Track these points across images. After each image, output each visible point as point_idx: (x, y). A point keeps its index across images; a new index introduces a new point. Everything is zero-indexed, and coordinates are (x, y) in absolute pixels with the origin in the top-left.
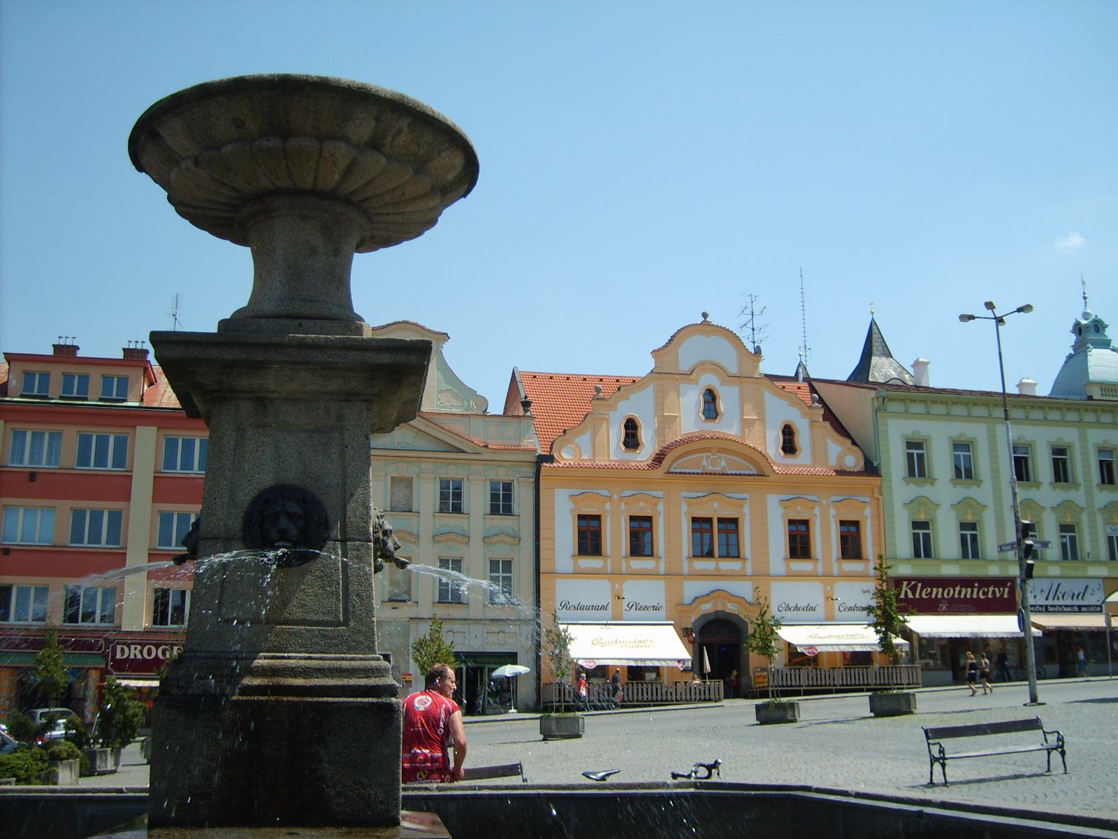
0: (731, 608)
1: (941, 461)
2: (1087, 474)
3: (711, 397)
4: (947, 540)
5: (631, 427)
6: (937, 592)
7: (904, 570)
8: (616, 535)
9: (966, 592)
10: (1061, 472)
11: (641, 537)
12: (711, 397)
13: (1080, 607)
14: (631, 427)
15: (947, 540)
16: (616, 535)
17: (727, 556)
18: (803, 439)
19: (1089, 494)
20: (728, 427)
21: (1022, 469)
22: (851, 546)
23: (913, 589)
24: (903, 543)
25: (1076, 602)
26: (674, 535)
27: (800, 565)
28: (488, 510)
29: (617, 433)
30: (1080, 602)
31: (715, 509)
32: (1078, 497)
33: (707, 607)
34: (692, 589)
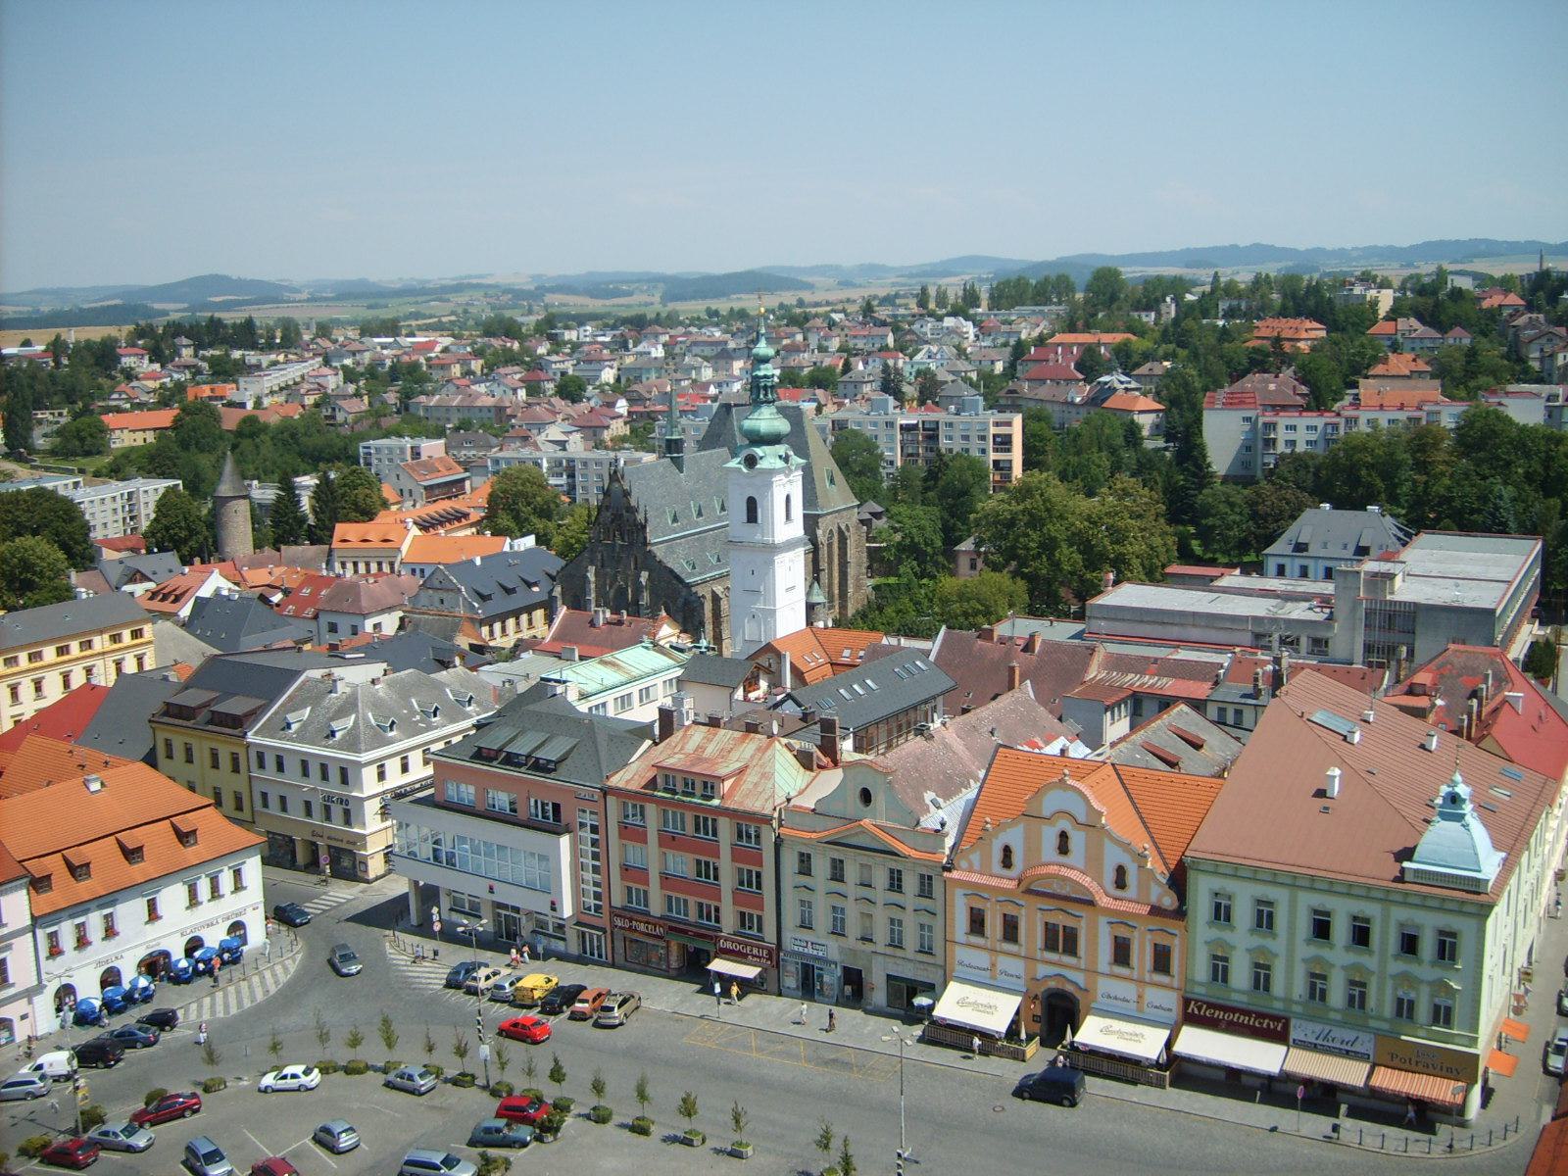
0: (1069, 988)
1: (1243, 913)
2: (1384, 942)
3: (1064, 836)
4: (1240, 976)
7: (1200, 990)
8: (994, 925)
10: (1361, 935)
11: (1011, 930)
12: (1064, 836)
13: (1348, 1052)
15: (1240, 976)
16: (994, 925)
17: (1065, 951)
19: (1383, 962)
21: (1322, 929)
22: (1162, 961)
23: (1199, 1009)
24: (1201, 971)
25: (1344, 1047)
26: (1032, 931)
28: (917, 891)
30: (1348, 1048)
31: (1060, 920)
32: (1370, 961)
33: (1052, 984)
34: (1042, 970)
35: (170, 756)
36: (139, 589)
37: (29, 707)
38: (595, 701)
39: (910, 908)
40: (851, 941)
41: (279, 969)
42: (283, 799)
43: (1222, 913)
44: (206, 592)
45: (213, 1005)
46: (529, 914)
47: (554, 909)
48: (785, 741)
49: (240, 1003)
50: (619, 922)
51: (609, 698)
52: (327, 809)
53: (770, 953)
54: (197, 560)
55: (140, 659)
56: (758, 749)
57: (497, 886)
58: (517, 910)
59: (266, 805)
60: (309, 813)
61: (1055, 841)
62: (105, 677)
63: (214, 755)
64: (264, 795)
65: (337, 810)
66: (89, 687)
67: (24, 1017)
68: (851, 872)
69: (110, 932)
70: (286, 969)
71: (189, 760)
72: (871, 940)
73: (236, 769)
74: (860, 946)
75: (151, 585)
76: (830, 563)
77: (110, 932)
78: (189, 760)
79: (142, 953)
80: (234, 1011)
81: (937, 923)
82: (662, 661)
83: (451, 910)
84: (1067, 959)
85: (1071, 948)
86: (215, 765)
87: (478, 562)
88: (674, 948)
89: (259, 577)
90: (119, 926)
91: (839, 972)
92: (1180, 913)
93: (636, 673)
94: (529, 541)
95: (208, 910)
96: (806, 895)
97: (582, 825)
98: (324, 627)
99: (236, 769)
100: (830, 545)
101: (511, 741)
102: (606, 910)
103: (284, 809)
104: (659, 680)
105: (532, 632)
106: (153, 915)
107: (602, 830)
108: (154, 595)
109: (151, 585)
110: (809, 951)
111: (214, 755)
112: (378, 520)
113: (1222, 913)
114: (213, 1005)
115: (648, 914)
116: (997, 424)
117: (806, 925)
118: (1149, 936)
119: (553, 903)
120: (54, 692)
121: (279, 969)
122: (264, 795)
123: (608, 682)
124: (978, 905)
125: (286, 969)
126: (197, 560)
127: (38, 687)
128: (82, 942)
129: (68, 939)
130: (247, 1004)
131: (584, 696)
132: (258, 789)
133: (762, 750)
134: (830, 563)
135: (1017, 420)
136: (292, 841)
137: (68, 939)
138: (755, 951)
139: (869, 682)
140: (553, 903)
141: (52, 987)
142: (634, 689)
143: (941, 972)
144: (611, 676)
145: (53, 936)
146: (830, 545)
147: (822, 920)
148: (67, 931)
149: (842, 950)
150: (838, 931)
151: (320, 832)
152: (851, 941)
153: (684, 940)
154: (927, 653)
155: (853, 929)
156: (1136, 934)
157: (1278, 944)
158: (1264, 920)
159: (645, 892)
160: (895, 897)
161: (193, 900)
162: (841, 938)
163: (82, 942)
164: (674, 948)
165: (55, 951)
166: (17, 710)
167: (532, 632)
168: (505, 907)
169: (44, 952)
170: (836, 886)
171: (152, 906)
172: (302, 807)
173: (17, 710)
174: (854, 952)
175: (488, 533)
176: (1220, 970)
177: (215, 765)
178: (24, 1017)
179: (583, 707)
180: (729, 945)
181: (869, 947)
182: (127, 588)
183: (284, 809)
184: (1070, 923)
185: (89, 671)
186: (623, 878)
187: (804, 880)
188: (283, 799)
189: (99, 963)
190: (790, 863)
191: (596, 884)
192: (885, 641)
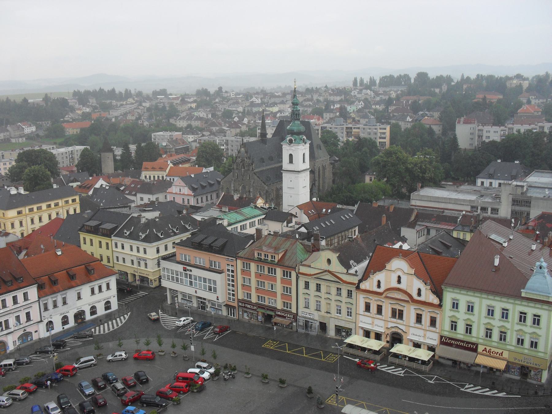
0: (400, 331)
3: (399, 277)
4: (461, 328)
5: (379, 282)
6: (453, 342)
7: (446, 334)
8: (373, 308)
9: (462, 344)
11: (379, 310)
12: (399, 277)
14: (379, 282)
16: (373, 308)
17: (398, 319)
18: (423, 293)
20: (402, 286)
22: (433, 322)
23: (446, 340)
24: (447, 326)
27: (418, 325)
28: (347, 296)
29: (376, 284)
31: (398, 307)
33: (394, 330)
34: (390, 325)
35: (85, 243)
36: (75, 185)
37: (37, 225)
38: (233, 226)
39: (344, 302)
40: (323, 313)
41: (122, 318)
42: (124, 259)
43: (455, 306)
44: (97, 186)
45: (100, 330)
46: (209, 301)
47: (218, 299)
48: (300, 241)
49: (109, 329)
50: (240, 304)
51: (239, 225)
52: (139, 263)
53: (294, 317)
54: (95, 175)
55: (75, 210)
56: (291, 244)
57: (198, 290)
58: (205, 299)
59: (118, 261)
60: (133, 264)
61: (396, 279)
62: (64, 216)
63: (100, 242)
64: (117, 257)
65: (142, 263)
66: (57, 219)
67: (36, 332)
68: (323, 288)
69: (65, 303)
70: (125, 318)
71: (92, 245)
72: (329, 313)
73: (108, 248)
74: (326, 315)
75: (79, 183)
76: (319, 178)
77: (65, 303)
78: (92, 245)
79: (76, 311)
80: (107, 331)
81: (354, 308)
82: (258, 212)
83: (182, 299)
84: (399, 321)
85: (401, 316)
86: (101, 247)
87: (193, 176)
88: (260, 314)
89: (116, 181)
90: (68, 301)
91: (318, 324)
92: (440, 306)
93: (249, 216)
94: (212, 169)
95: (98, 296)
96: (307, 296)
97: (228, 270)
98: (139, 199)
99: (108, 248)
100: (319, 172)
101: (204, 240)
102: (236, 300)
103: (124, 262)
104: (256, 219)
105: (212, 201)
106: (79, 298)
107: (235, 272)
108: (80, 187)
109: (79, 183)
110: (308, 316)
111: (100, 242)
112: (158, 161)
113: (455, 306)
114: (100, 330)
115: (251, 302)
116: (381, 129)
117: (307, 307)
118: (429, 314)
119: (218, 297)
120: (46, 221)
121: (122, 318)
122: (117, 257)
123: (238, 220)
124: (368, 301)
125: (125, 318)
126: (95, 175)
127: (40, 219)
128: (55, 306)
129: (50, 306)
130: (111, 329)
131: (230, 225)
132: (115, 255)
133: (292, 244)
134: (319, 178)
135: (388, 128)
136: (127, 274)
137: (50, 306)
138: (289, 316)
139: (331, 221)
140: (218, 297)
141: (46, 321)
142: (248, 222)
143: (354, 324)
144: (240, 218)
145: (46, 305)
146: (319, 172)
147: (313, 305)
148: (50, 301)
149: (319, 316)
150: (318, 310)
151: (136, 270)
152: (323, 313)
153: (263, 311)
154: (352, 211)
155: (324, 308)
156: (424, 313)
157: (474, 318)
158: (470, 308)
159: (250, 294)
160: (338, 298)
162: (319, 312)
163: (55, 306)
164: (260, 314)
165: (46, 309)
166: (33, 226)
167: (212, 201)
168: (201, 298)
170: (318, 294)
171: (79, 294)
172: (130, 262)
173: (33, 226)
174: (323, 317)
175: (197, 166)
176: (454, 326)
177: (101, 247)
178: (36, 332)
179: (229, 228)
180: (279, 313)
181: (329, 315)
182: (71, 184)
183: (124, 262)
184: (401, 308)
185: (57, 214)
186: (242, 289)
187: (306, 291)
188: (124, 259)
189: (61, 314)
190: (302, 284)
191: (233, 291)
192: (338, 206)
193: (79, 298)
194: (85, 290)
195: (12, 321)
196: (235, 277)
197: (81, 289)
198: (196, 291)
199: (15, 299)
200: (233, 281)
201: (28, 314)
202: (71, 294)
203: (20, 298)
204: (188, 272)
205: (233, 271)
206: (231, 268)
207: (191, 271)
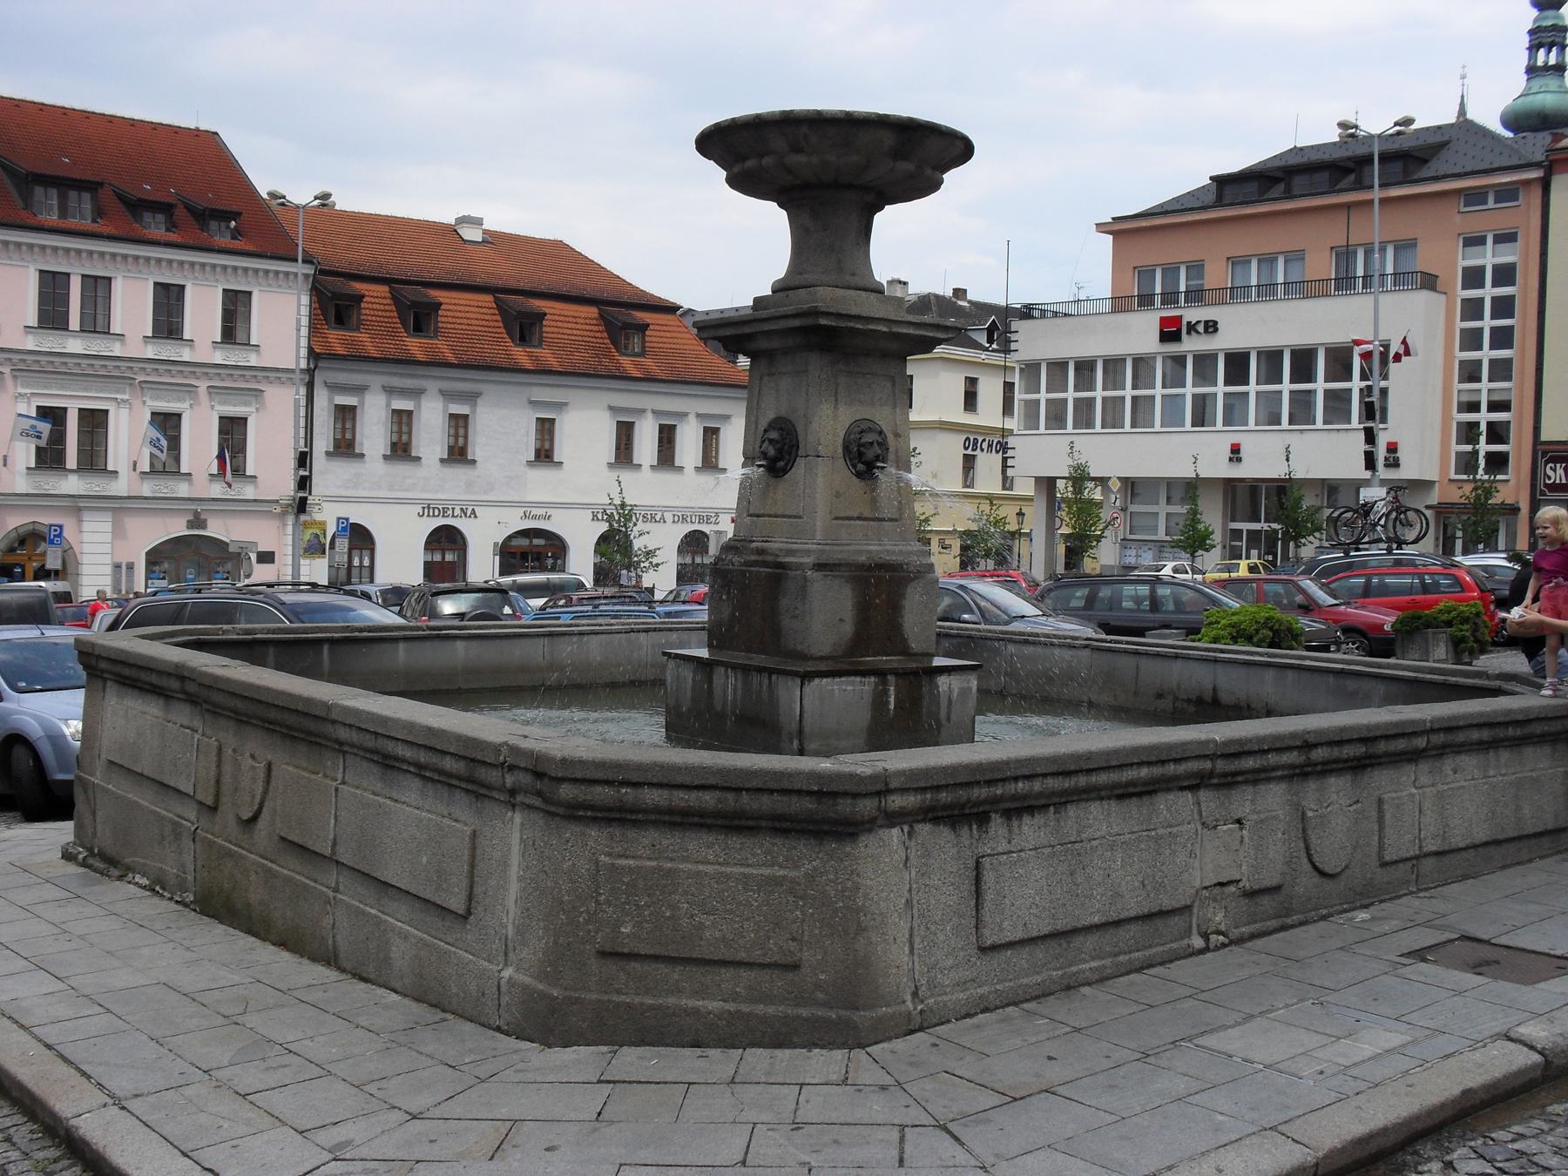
57: (1249, 444)
69: (458, 454)
77: (458, 454)
90: (477, 450)
106: (544, 456)
128: (401, 450)
129: (373, 433)
137: (373, 433)
161: (624, 452)
165: (345, 448)
169: (322, 443)
171: (546, 428)
189: (429, 509)
193: (544, 456)
194: (586, 426)
195: (128, 436)
196: (1522, 291)
197: (561, 406)
198: (1235, 449)
199: (169, 303)
200: (1502, 338)
201: (232, 432)
202: (502, 423)
203: (202, 311)
204: (1191, 345)
205: (1504, 275)
206: (1489, 257)
207: (1211, 327)
